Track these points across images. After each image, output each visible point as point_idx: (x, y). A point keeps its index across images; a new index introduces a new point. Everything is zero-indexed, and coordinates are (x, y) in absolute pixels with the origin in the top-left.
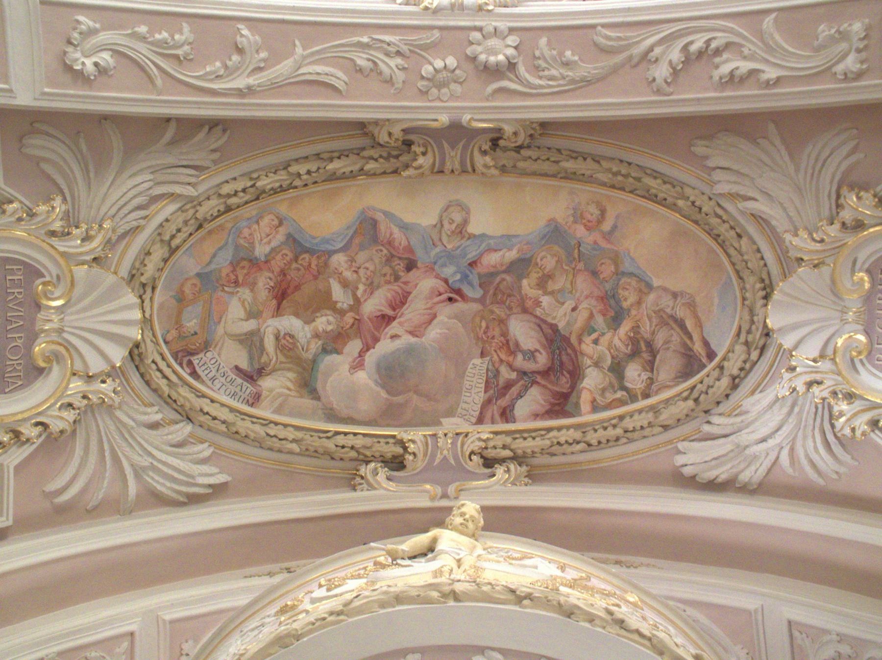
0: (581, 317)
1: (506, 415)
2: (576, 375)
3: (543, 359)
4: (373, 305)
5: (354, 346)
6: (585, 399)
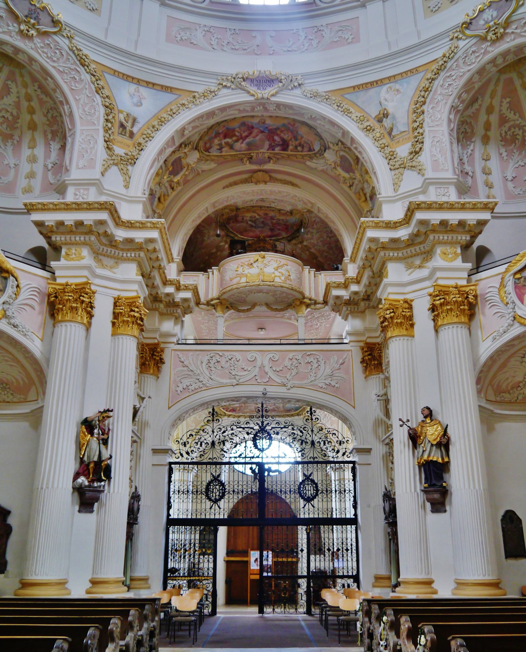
0: (289, 138)
1: (273, 150)
2: (288, 146)
3: (281, 143)
4: (244, 135)
5: (241, 141)
6: (289, 150)
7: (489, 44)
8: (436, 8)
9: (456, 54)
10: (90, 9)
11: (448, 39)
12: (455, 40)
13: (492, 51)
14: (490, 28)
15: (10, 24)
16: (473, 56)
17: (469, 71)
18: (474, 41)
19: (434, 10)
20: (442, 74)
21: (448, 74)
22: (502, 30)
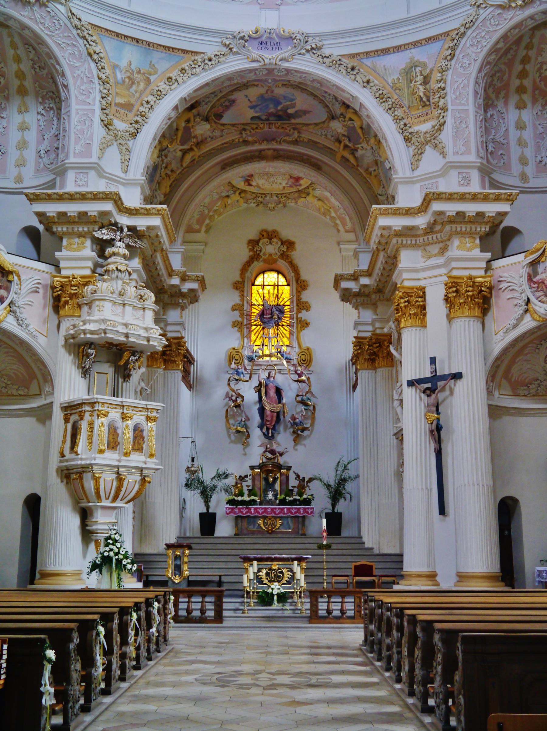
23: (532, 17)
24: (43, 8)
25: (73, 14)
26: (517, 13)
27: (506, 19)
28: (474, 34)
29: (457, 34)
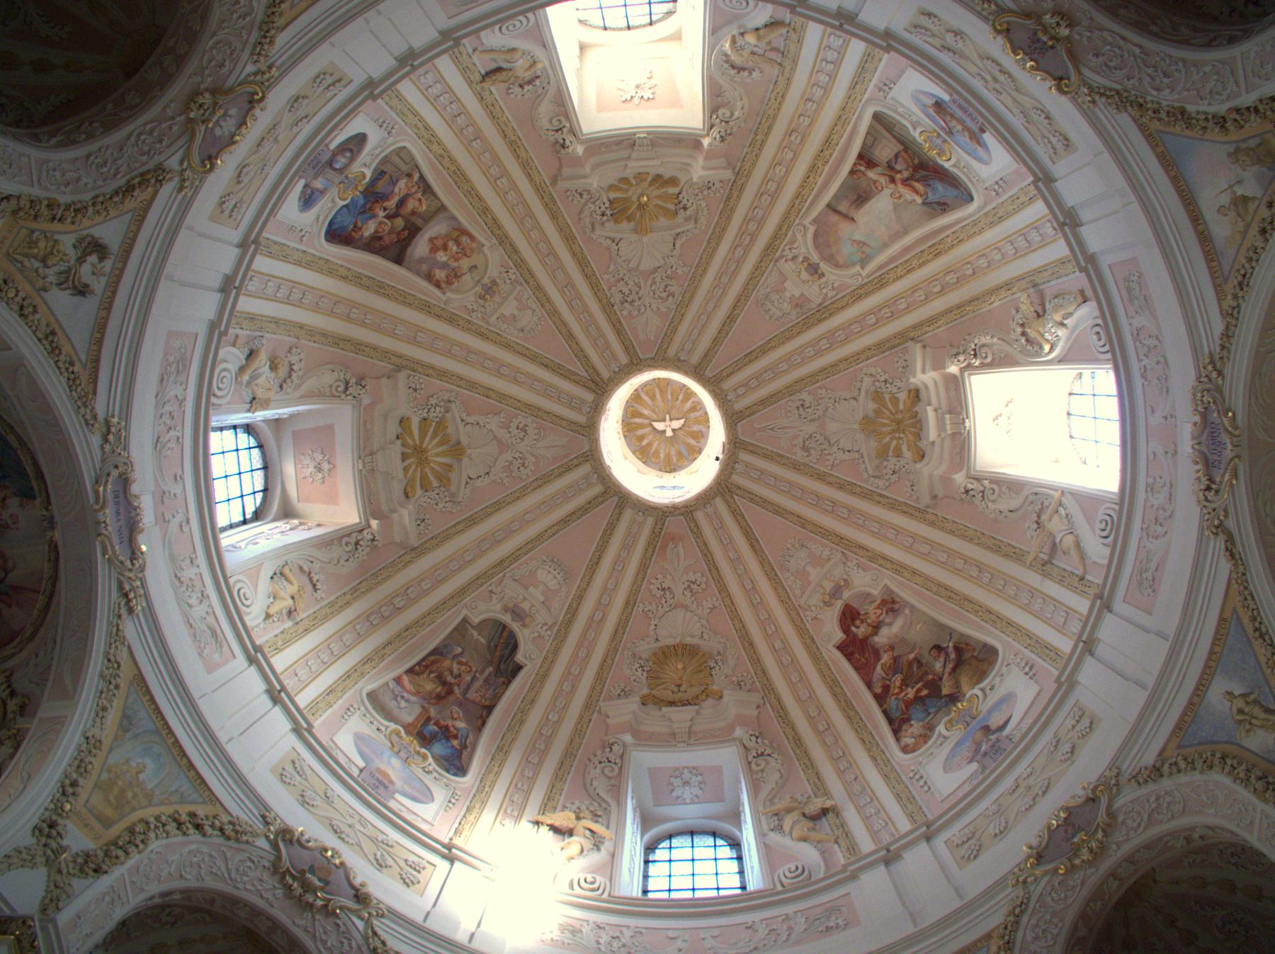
7: (202, 87)
8: (318, 80)
9: (252, 54)
10: (935, 17)
11: (277, 64)
12: (264, 68)
13: (190, 77)
14: (214, 112)
15: (1085, 39)
16: (219, 58)
17: (214, 34)
18: (230, 83)
19: (322, 76)
20: (260, 17)
21: (248, 19)
22: (192, 115)
23: (1113, 874)
24: (331, 920)
25: (375, 933)
26: (1089, 872)
27: (1074, 887)
28: (1034, 921)
29: (1006, 928)
